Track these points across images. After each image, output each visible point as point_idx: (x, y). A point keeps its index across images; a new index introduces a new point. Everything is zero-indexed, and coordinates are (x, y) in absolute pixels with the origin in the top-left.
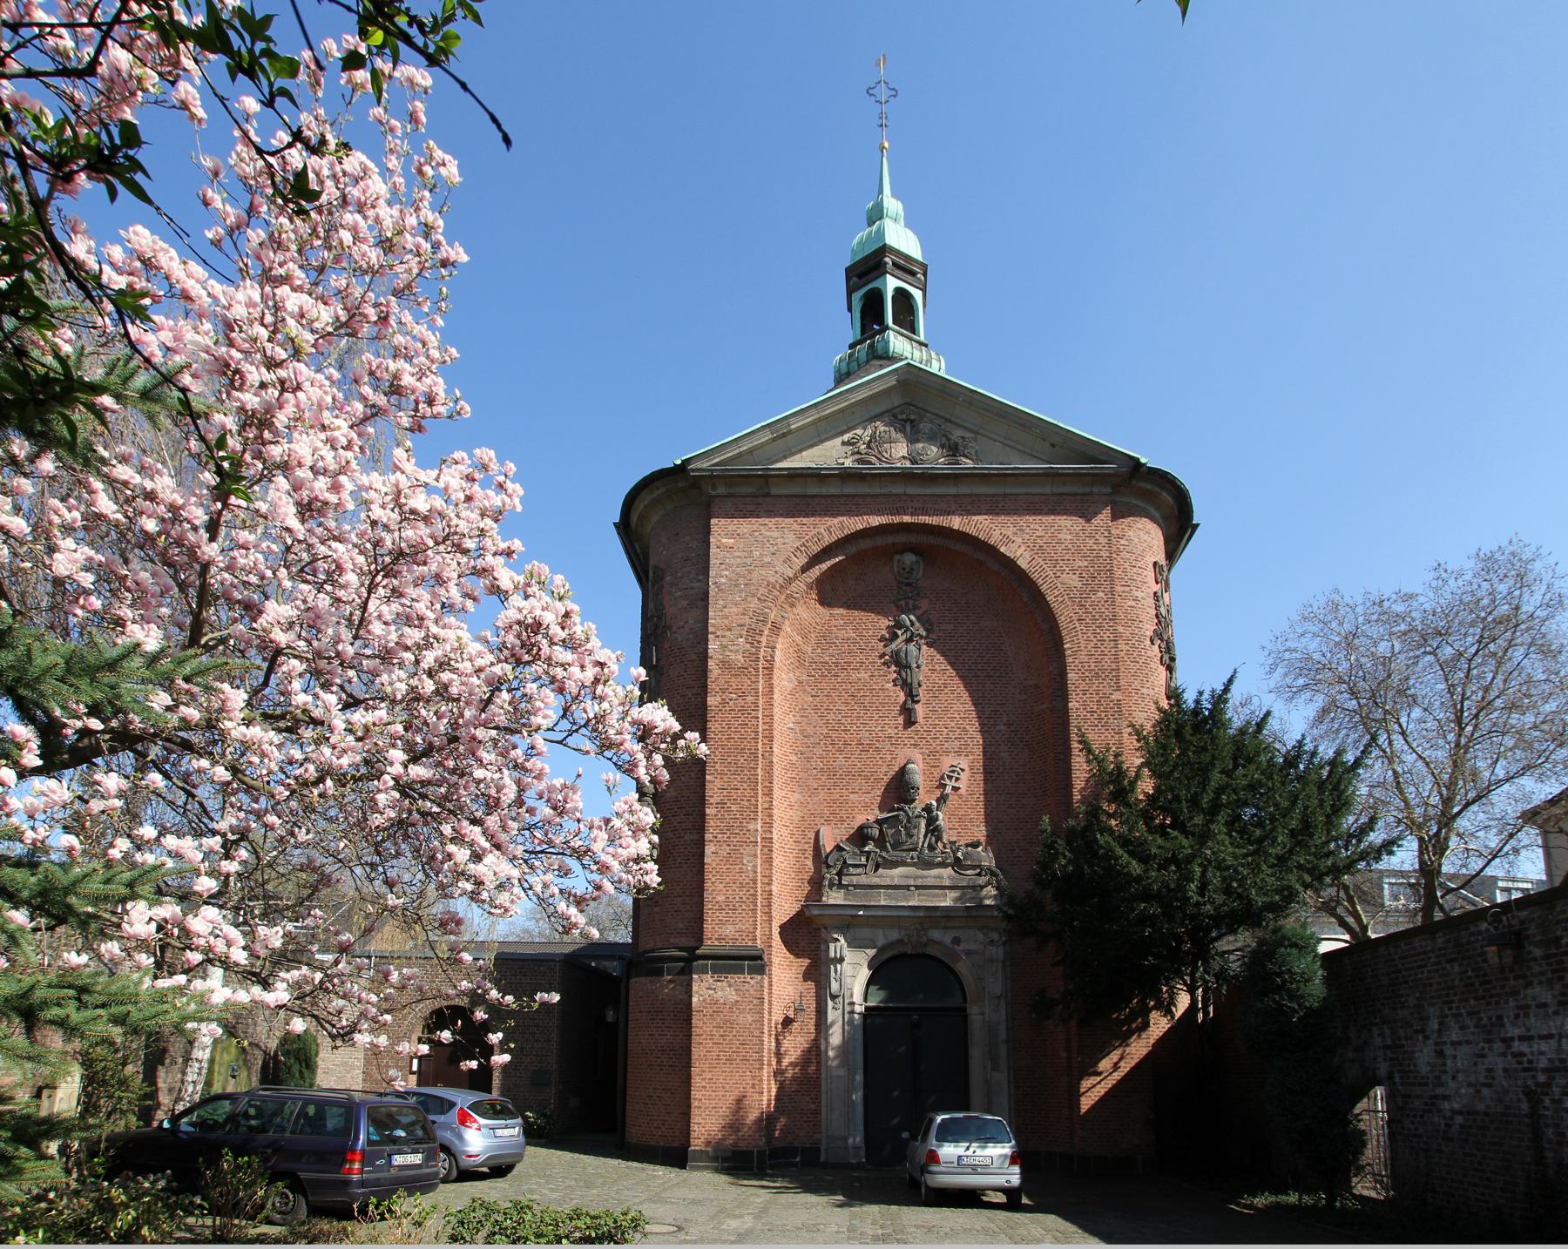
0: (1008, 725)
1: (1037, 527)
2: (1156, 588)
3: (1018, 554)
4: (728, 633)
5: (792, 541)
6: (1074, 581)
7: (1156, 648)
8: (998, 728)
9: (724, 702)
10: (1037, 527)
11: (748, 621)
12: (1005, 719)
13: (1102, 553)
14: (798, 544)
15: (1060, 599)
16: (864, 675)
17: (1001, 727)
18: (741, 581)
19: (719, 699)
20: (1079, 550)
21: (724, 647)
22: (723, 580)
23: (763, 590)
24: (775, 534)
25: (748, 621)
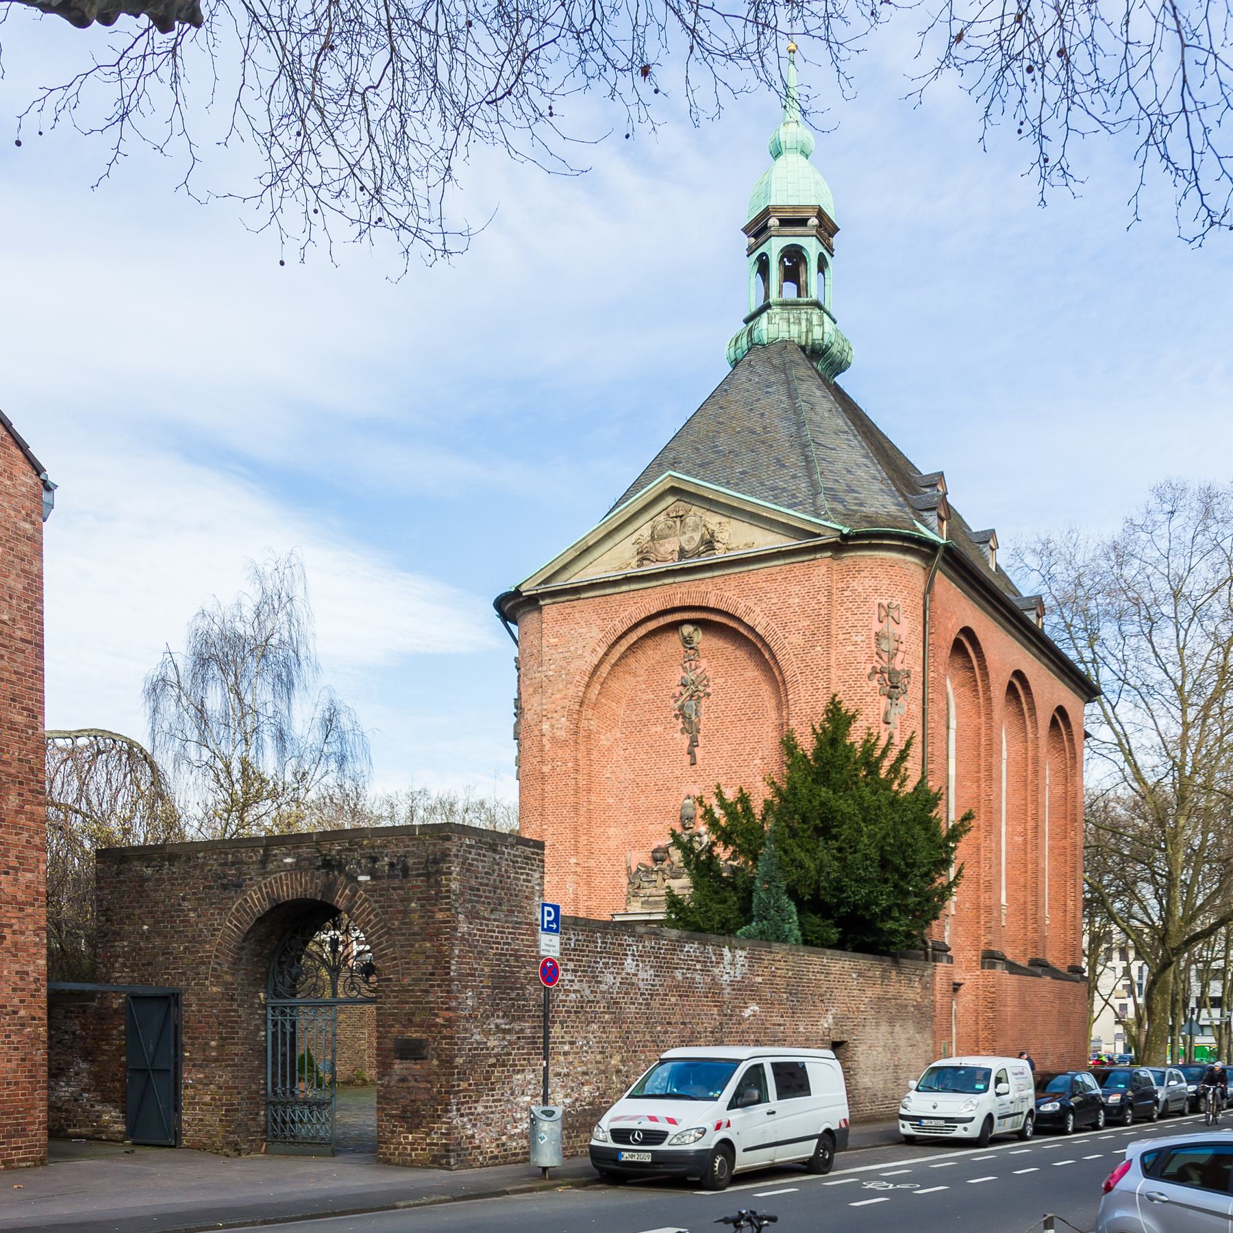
0: (763, 758)
1: (773, 595)
2: (877, 627)
3: (757, 623)
4: (555, 715)
5: (596, 634)
6: (797, 639)
7: (875, 683)
8: (755, 762)
9: (553, 769)
10: (773, 595)
11: (568, 703)
12: (760, 754)
13: (822, 612)
14: (601, 636)
15: (787, 657)
16: (660, 729)
17: (758, 761)
18: (563, 672)
19: (550, 767)
20: (804, 612)
21: (552, 726)
22: (551, 673)
23: (578, 678)
24: (584, 631)
25: (568, 703)
